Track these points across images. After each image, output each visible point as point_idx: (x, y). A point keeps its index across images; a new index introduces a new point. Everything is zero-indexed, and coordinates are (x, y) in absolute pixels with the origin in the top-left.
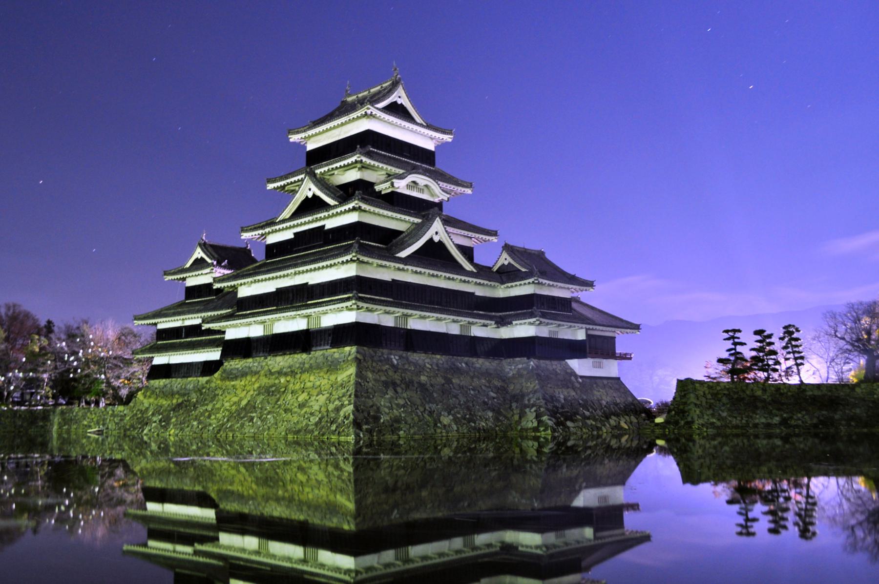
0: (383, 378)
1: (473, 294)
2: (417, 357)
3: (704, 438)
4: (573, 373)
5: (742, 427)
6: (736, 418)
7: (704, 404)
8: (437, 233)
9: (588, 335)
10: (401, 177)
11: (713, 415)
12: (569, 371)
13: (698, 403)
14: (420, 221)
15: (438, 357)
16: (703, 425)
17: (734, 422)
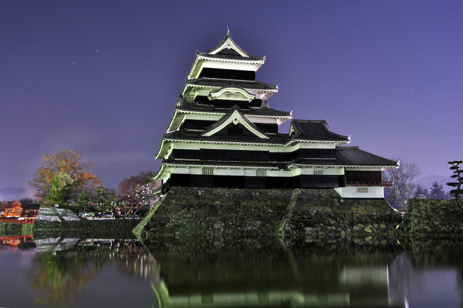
0: (185, 203)
1: (268, 152)
2: (219, 191)
3: (417, 240)
4: (339, 197)
5: (448, 233)
6: (445, 226)
7: (423, 216)
8: (236, 120)
9: (346, 172)
10: (217, 91)
11: (428, 224)
12: (334, 195)
13: (419, 215)
14: (225, 114)
15: (238, 190)
16: (417, 231)
17: (443, 228)
